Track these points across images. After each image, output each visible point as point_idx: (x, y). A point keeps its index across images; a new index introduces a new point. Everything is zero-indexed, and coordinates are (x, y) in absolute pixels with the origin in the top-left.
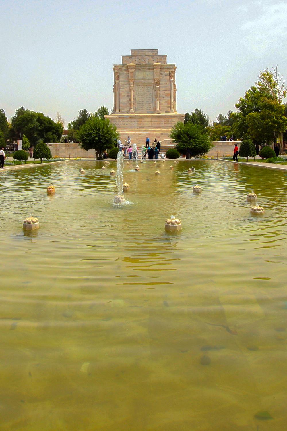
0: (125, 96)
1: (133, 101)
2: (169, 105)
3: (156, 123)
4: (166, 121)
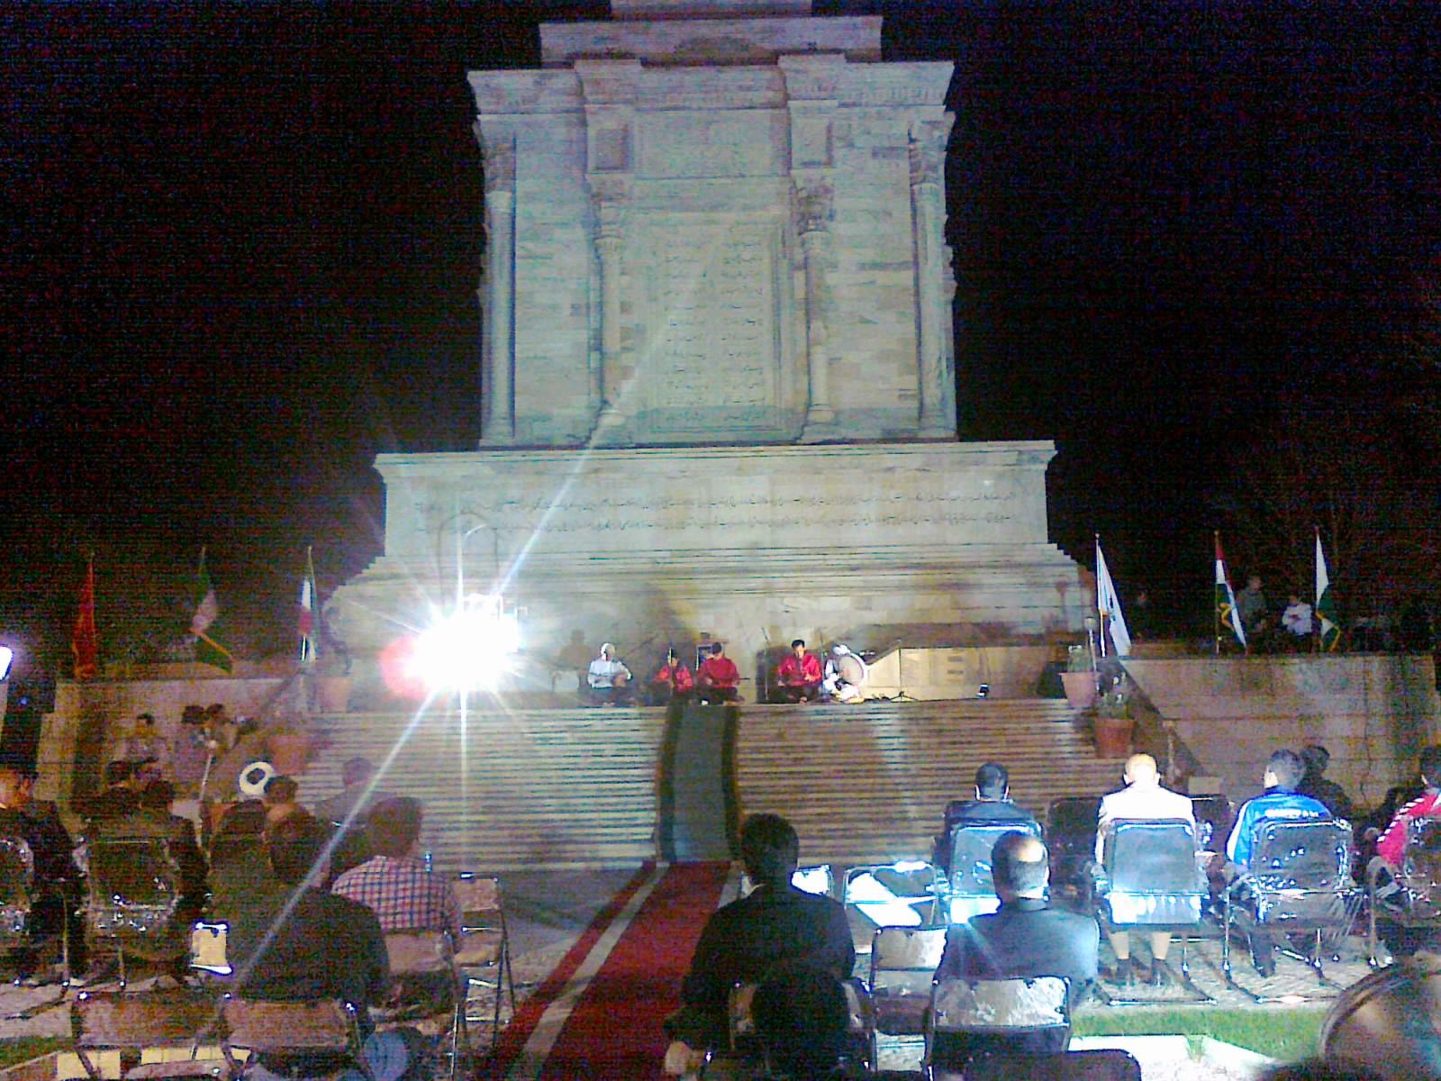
0: (554, 307)
4: (892, 494)
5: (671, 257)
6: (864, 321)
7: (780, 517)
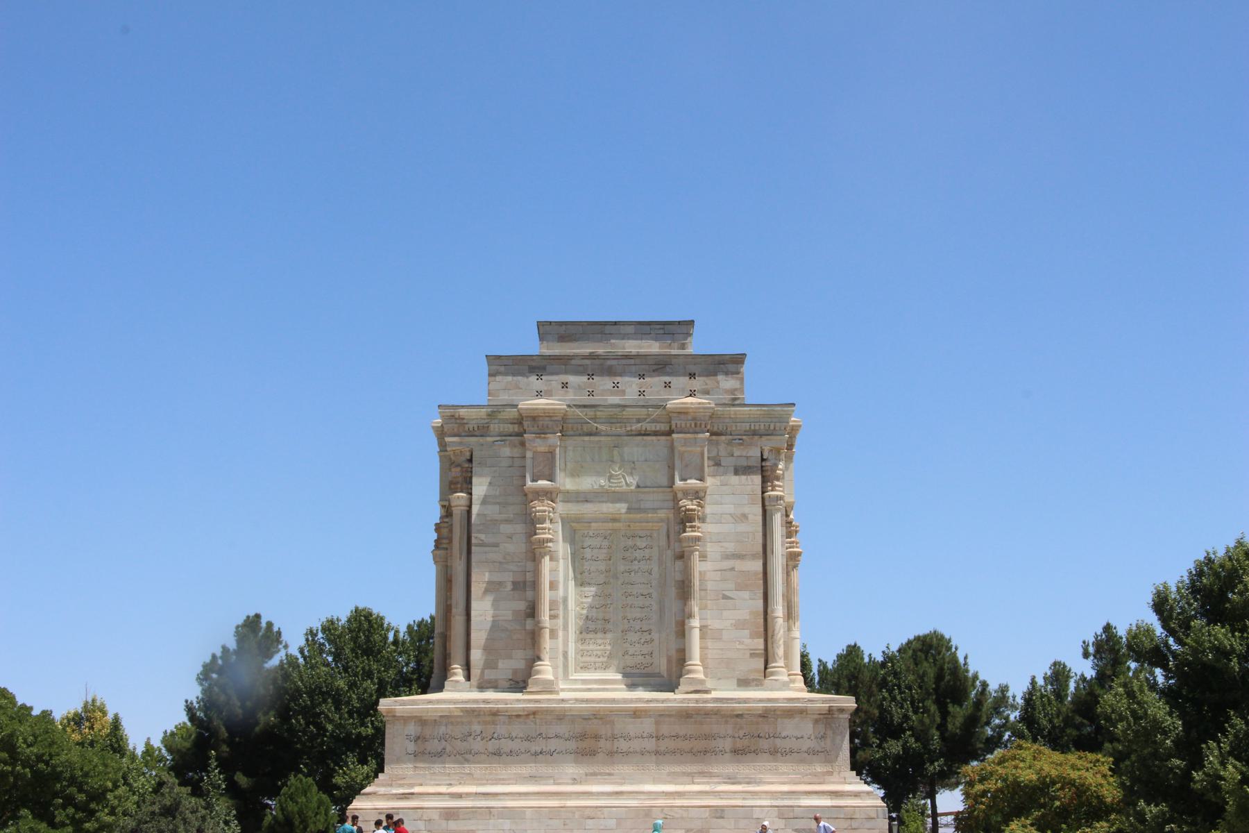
0: (500, 583)
1: (552, 617)
2: (761, 641)
4: (741, 733)
5: (586, 545)
6: (725, 597)
7: (663, 748)
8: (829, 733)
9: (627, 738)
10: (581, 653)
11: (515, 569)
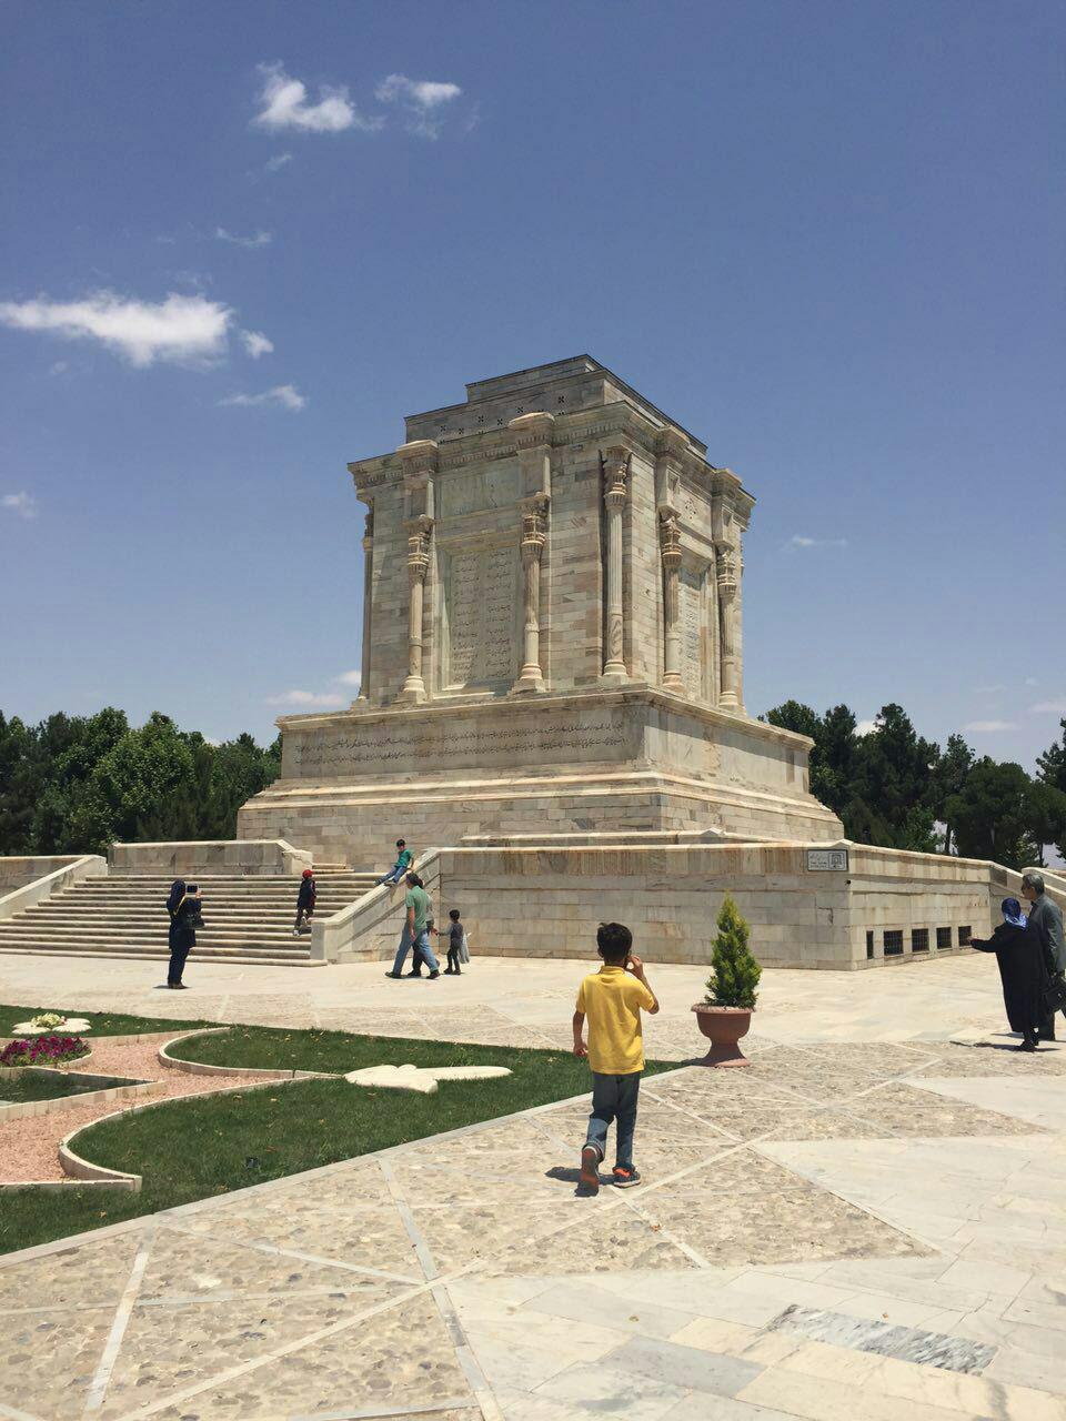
0: (391, 611)
1: (424, 636)
3: (503, 742)
8: (627, 721)
9: (455, 738)
10: (454, 666)
11: (402, 596)
